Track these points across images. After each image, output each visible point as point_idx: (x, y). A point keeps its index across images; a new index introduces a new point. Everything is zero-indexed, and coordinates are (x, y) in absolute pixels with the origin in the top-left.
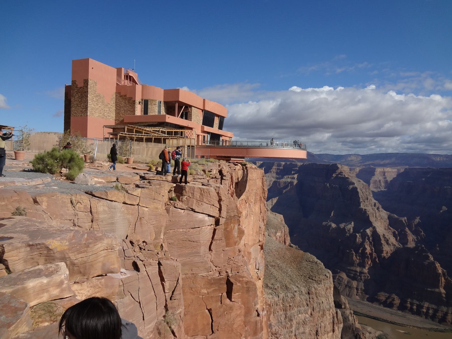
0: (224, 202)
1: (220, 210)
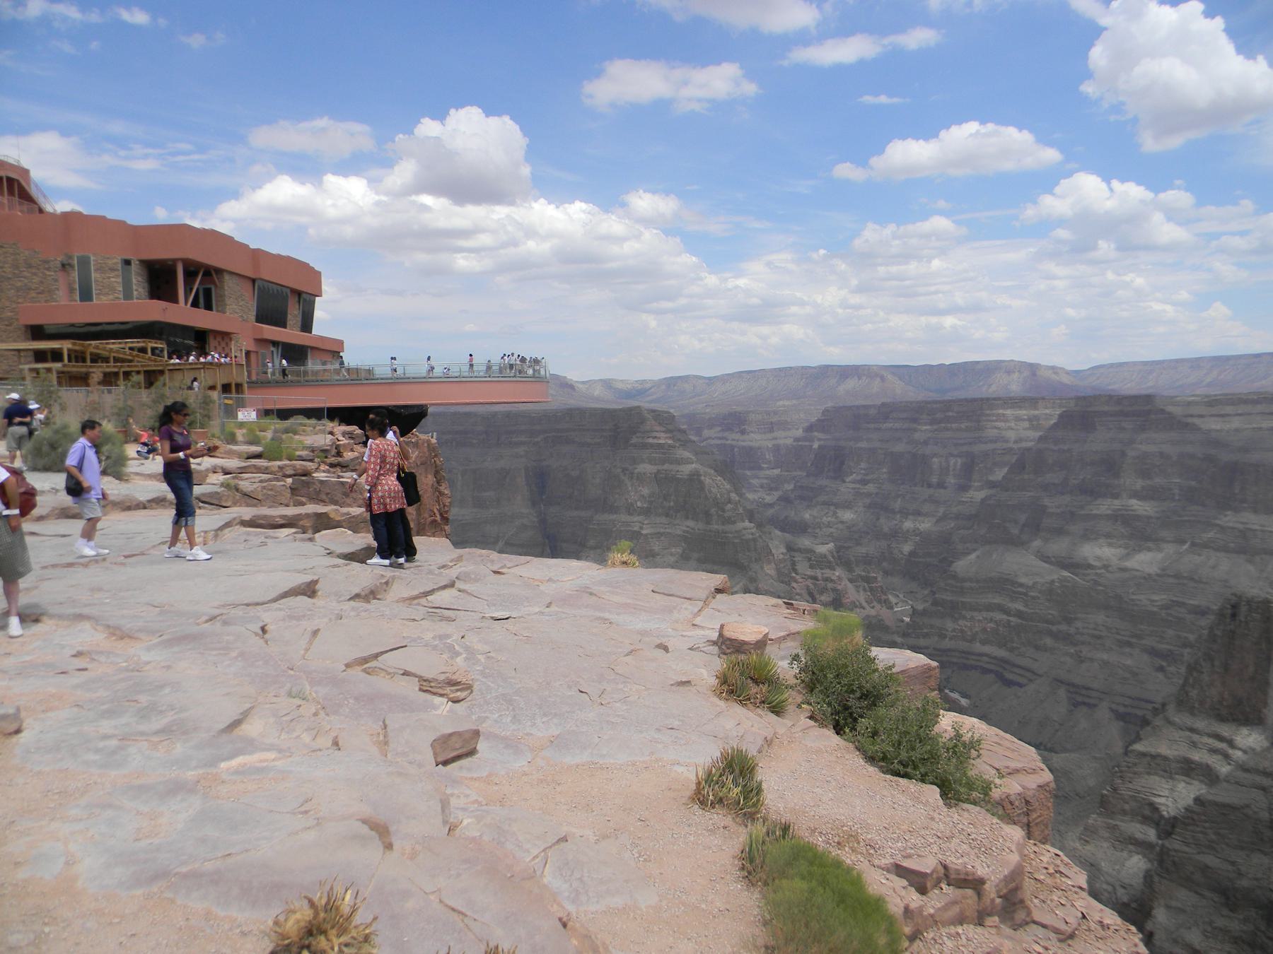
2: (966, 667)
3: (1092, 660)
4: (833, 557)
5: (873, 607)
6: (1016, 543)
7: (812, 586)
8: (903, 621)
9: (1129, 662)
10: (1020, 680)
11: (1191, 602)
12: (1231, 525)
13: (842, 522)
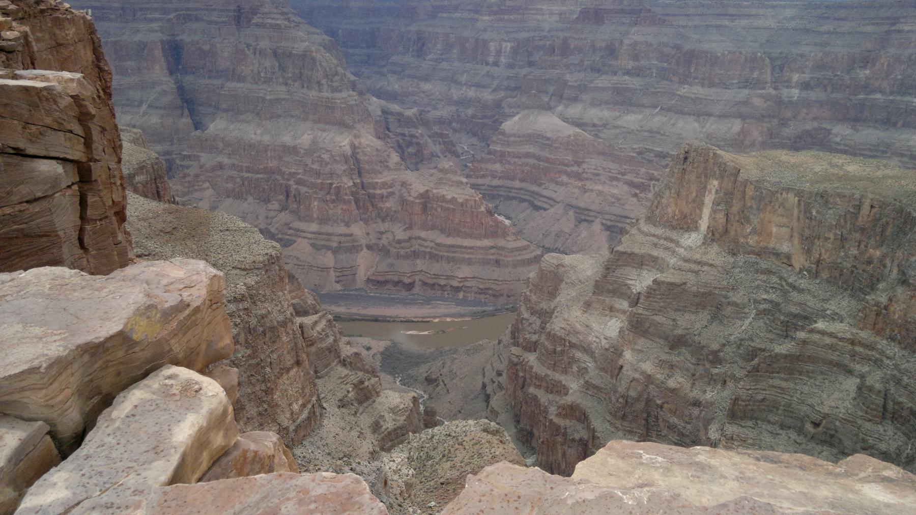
0: (95, 120)
1: (88, 142)
2: (510, 198)
3: (592, 190)
4: (417, 118)
5: (446, 156)
6: (549, 108)
7: (401, 141)
8: (466, 166)
9: (615, 191)
11: (658, 149)
12: (686, 95)
13: (424, 92)
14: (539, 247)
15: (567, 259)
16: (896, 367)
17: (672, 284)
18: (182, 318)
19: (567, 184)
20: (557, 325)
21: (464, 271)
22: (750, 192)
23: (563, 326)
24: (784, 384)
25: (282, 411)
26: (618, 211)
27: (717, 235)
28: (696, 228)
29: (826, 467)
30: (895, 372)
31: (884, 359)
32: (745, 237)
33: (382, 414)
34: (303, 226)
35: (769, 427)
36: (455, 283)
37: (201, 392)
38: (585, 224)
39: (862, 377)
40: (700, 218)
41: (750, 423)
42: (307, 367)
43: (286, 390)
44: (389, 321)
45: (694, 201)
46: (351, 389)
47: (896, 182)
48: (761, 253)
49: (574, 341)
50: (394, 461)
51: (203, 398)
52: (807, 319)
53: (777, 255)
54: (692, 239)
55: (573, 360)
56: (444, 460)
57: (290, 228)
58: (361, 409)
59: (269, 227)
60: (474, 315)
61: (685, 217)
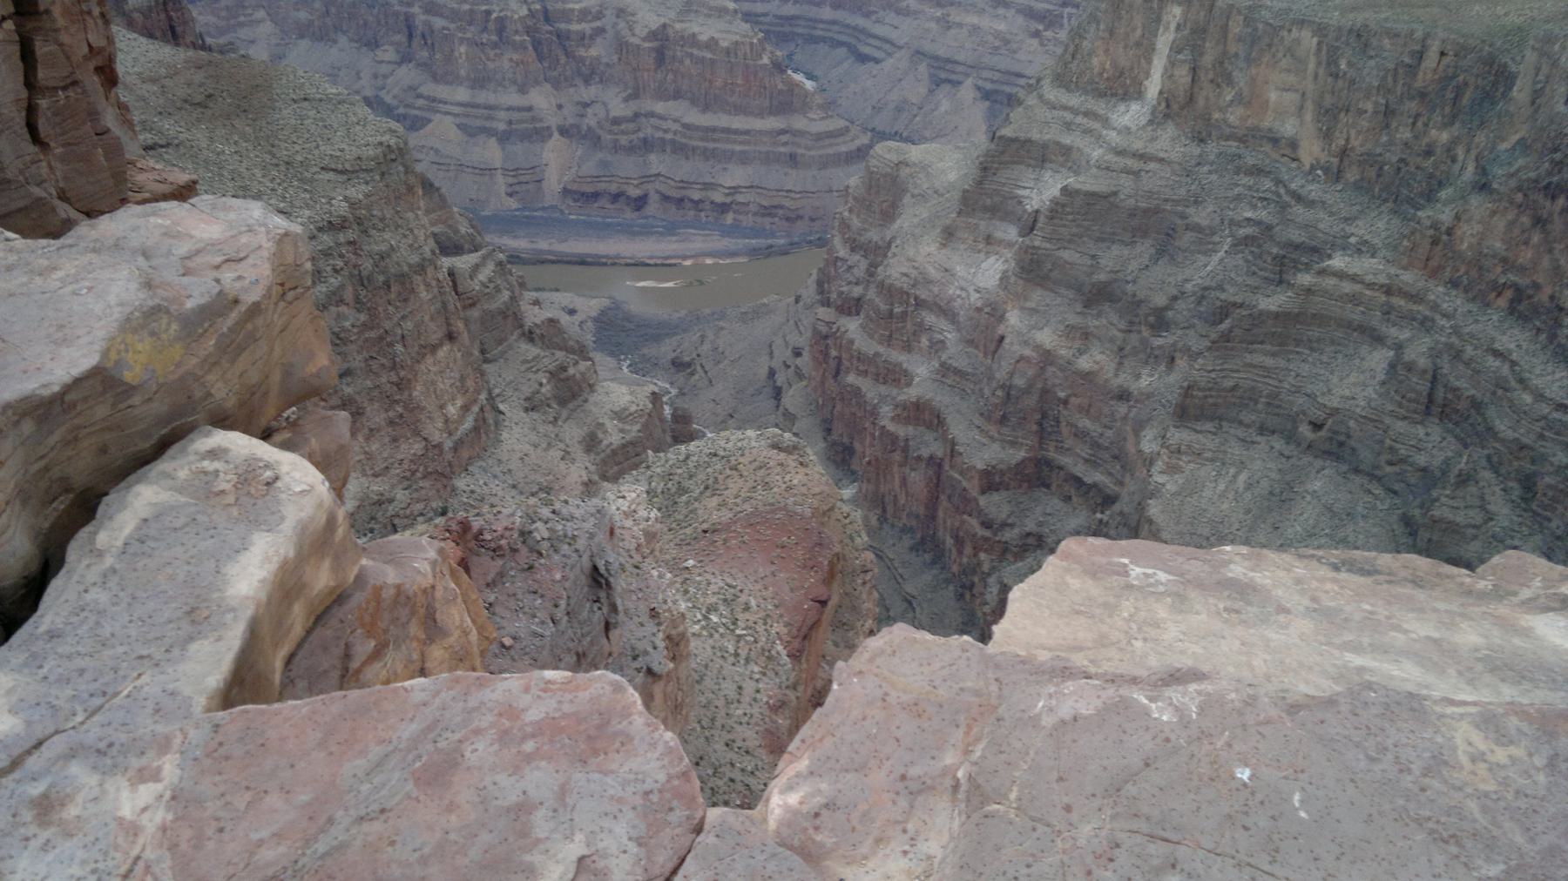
3: (960, 25)
9: (1002, 27)
10: (878, 54)
14: (865, 130)
15: (915, 153)
16: (1456, 330)
17: (1093, 194)
18: (225, 330)
19: (916, 12)
20: (895, 270)
21: (736, 176)
22: (1236, 27)
23: (904, 270)
24: (1269, 362)
25: (429, 418)
26: (1004, 63)
27: (1175, 107)
28: (1139, 95)
29: (1459, 580)
30: (1454, 339)
31: (1437, 317)
32: (1222, 110)
33: (601, 421)
34: (442, 91)
35: (1241, 432)
36: (718, 197)
37: (279, 484)
38: (946, 88)
39: (1399, 347)
40: (1148, 75)
41: (1209, 426)
42: (467, 342)
43: (433, 383)
44: (605, 264)
45: (1138, 44)
46: (544, 381)
47: (1489, 8)
48: (1249, 137)
49: (923, 297)
50: (624, 497)
51: (283, 496)
52: (1317, 252)
53: (1275, 141)
54: (1131, 115)
55: (921, 328)
56: (708, 493)
57: (419, 96)
58: (565, 413)
59: (382, 94)
60: (754, 253)
61: (1122, 73)
